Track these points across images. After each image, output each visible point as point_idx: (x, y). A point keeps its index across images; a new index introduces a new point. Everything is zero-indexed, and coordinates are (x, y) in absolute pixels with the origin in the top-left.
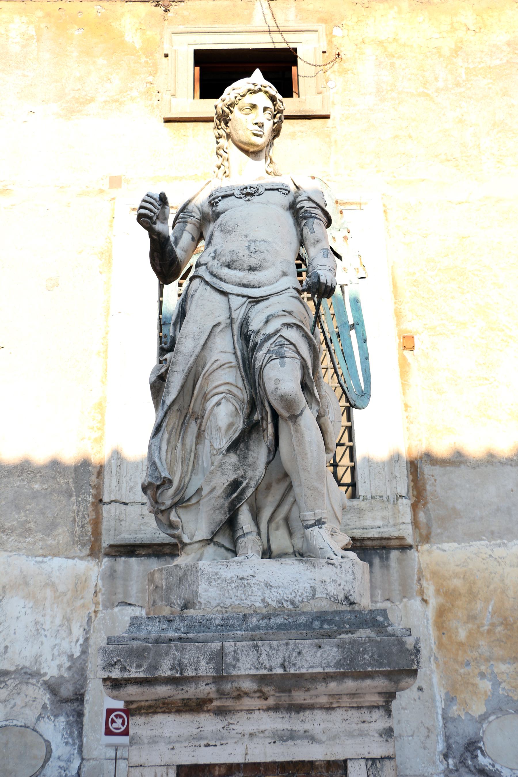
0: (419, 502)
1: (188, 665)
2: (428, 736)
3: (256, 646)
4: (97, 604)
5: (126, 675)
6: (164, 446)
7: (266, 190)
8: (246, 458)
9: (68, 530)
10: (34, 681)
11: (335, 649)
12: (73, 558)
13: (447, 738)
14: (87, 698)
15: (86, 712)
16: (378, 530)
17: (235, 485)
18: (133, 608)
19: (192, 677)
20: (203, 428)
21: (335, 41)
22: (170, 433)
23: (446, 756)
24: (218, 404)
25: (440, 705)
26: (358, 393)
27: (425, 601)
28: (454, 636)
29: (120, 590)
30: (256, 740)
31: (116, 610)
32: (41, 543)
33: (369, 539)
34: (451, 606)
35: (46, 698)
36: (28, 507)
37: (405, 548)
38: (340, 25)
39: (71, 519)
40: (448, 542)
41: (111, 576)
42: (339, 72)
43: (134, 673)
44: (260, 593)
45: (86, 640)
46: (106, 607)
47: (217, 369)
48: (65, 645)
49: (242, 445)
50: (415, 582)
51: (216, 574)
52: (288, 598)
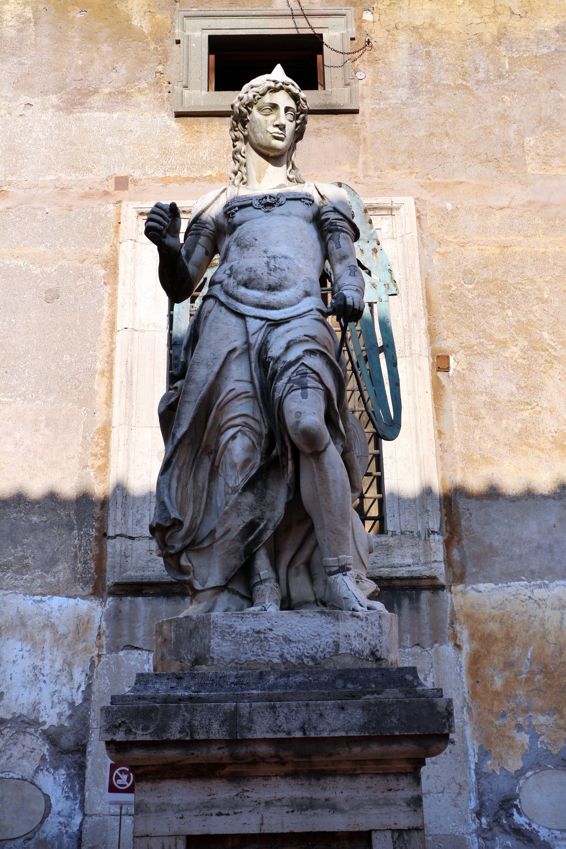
0: (453, 538)
1: (199, 727)
2: (460, 793)
3: (273, 708)
4: (100, 647)
5: (131, 738)
6: (174, 484)
7: (287, 199)
8: (264, 497)
9: (69, 566)
10: (32, 730)
11: (360, 711)
12: (75, 597)
13: (480, 795)
14: (89, 749)
15: (89, 764)
16: (408, 569)
17: (251, 526)
18: (139, 652)
19: (203, 741)
20: (216, 464)
21: (365, 27)
22: (181, 470)
23: (479, 815)
24: (233, 437)
25: (473, 759)
26: (387, 423)
27: (458, 647)
28: (489, 684)
29: (125, 632)
30: (273, 809)
31: (121, 654)
32: (39, 581)
33: (398, 578)
34: (486, 652)
35: (45, 749)
36: (26, 541)
37: (436, 588)
38: (371, 9)
39: (73, 555)
40: (484, 583)
41: (115, 617)
42: (368, 61)
43: (140, 736)
44: (278, 649)
45: (89, 686)
46: (110, 651)
47: (232, 399)
48: (66, 691)
49: (259, 484)
50: (448, 626)
51: (230, 627)
52: (308, 653)
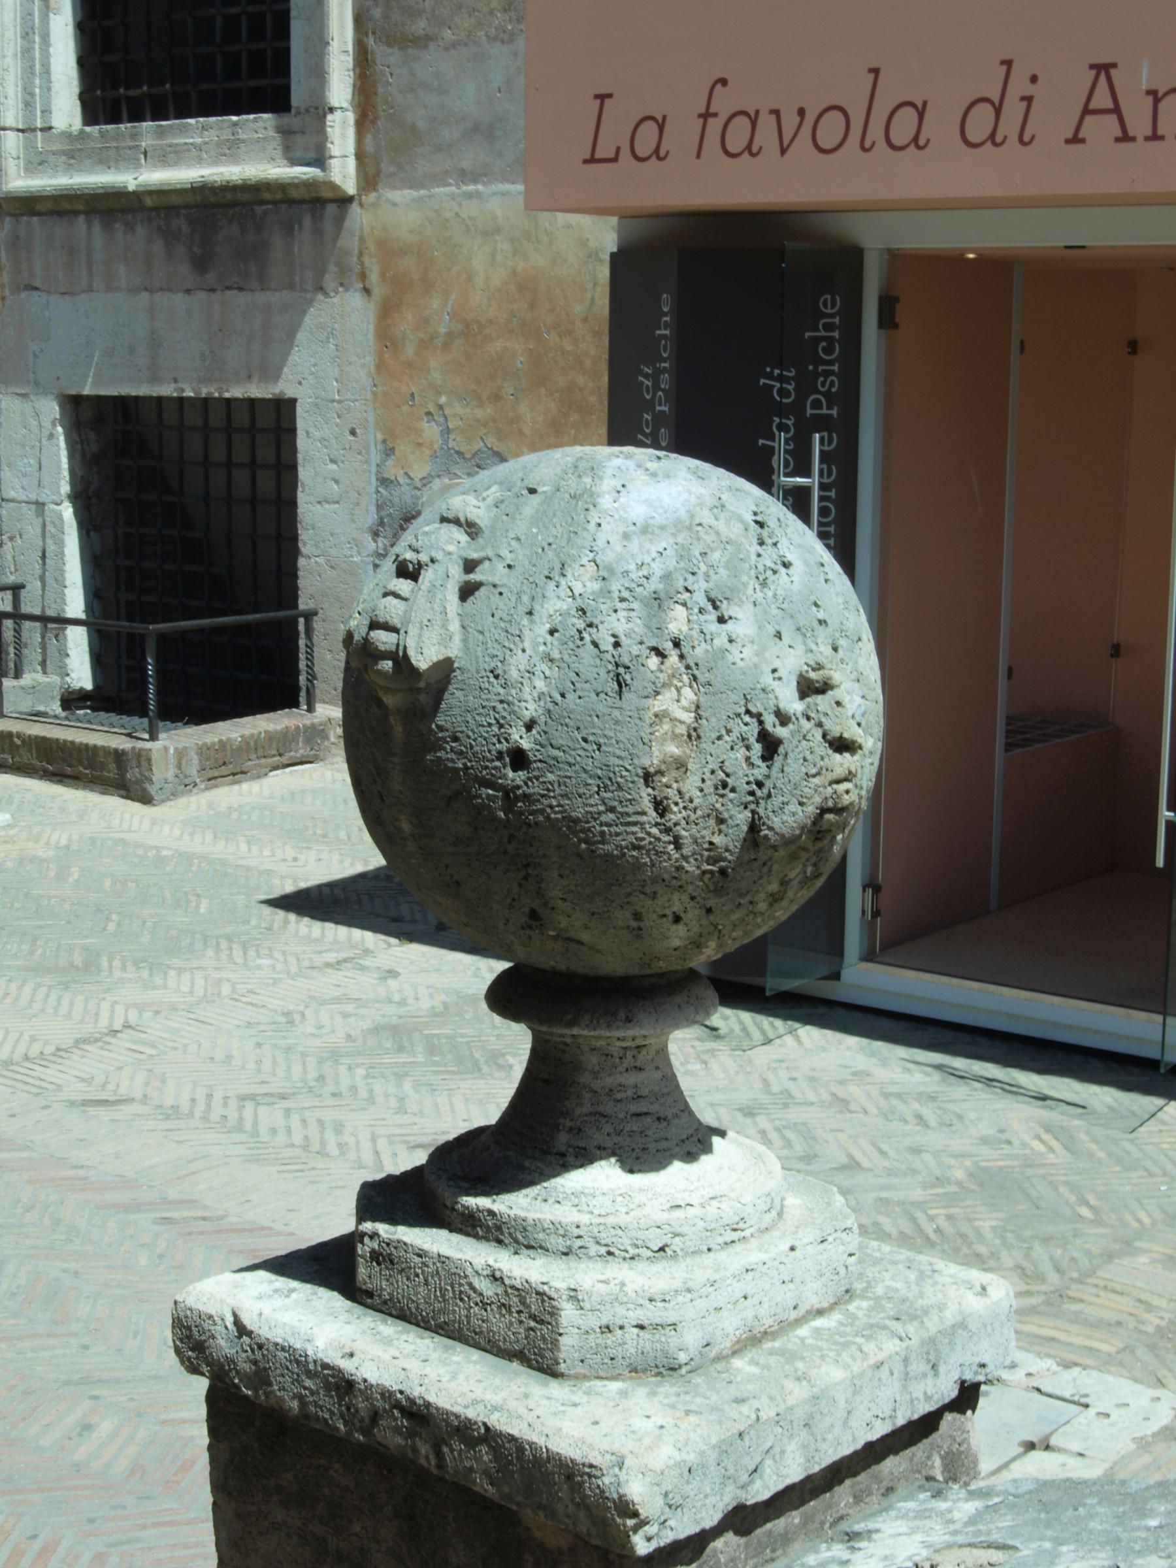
31: (23, 295)
50: (355, 259)
